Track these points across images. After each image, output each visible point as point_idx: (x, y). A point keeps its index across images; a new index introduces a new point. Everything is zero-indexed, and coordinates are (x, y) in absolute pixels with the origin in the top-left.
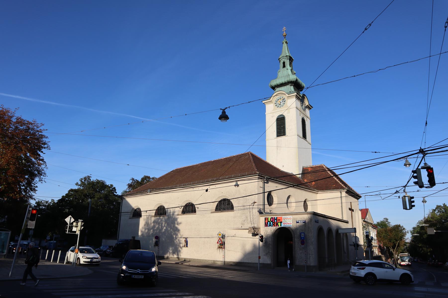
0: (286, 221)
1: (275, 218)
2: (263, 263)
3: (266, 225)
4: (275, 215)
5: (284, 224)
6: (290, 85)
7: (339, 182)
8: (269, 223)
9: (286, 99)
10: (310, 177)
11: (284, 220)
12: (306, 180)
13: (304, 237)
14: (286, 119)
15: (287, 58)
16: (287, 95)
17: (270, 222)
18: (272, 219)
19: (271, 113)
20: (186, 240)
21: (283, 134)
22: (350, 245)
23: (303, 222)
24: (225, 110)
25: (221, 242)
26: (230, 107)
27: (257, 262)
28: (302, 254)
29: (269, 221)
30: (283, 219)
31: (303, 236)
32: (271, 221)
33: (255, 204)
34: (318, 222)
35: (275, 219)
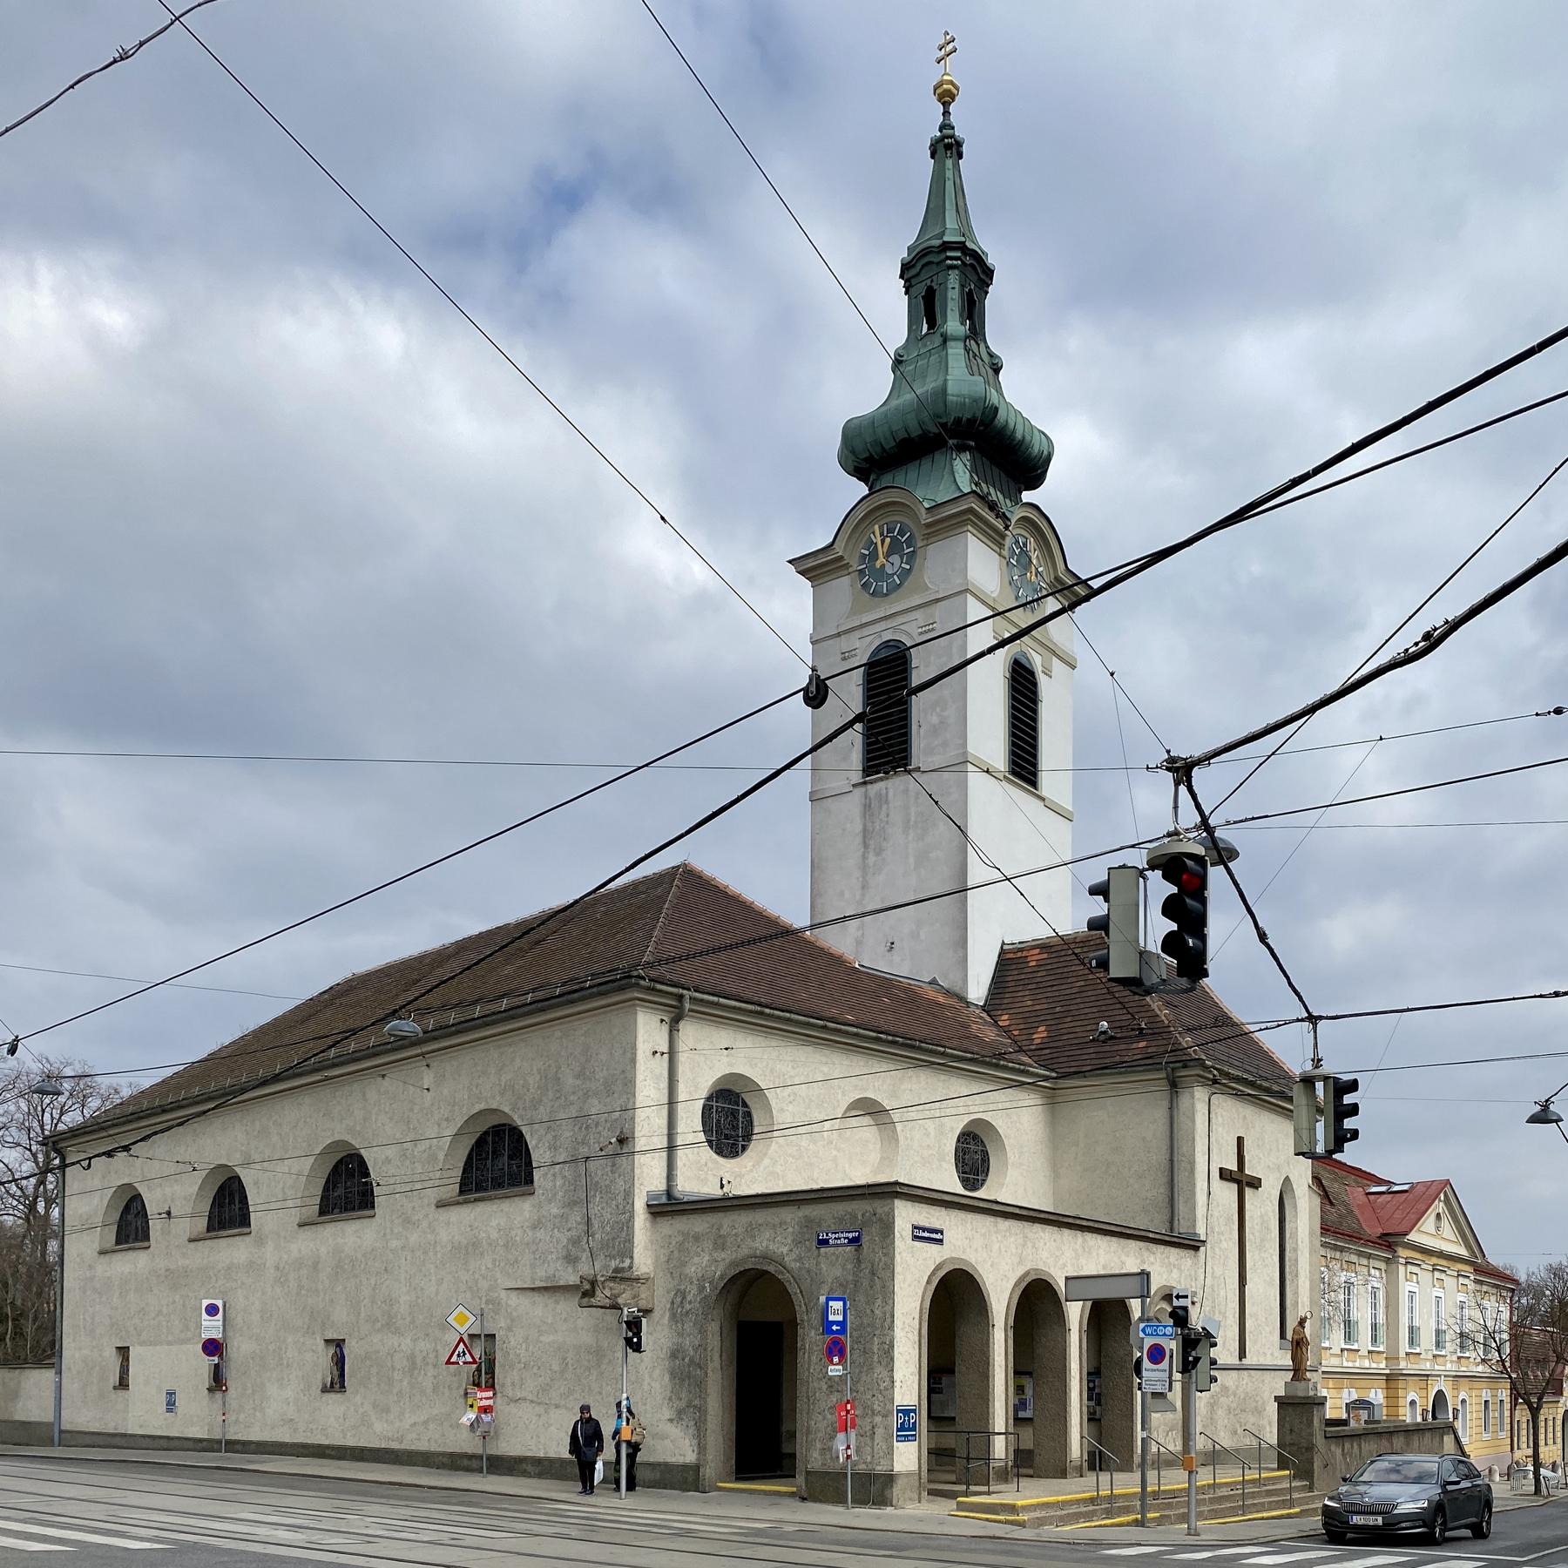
13: (842, 1324)
23: (852, 1241)
31: (840, 1318)
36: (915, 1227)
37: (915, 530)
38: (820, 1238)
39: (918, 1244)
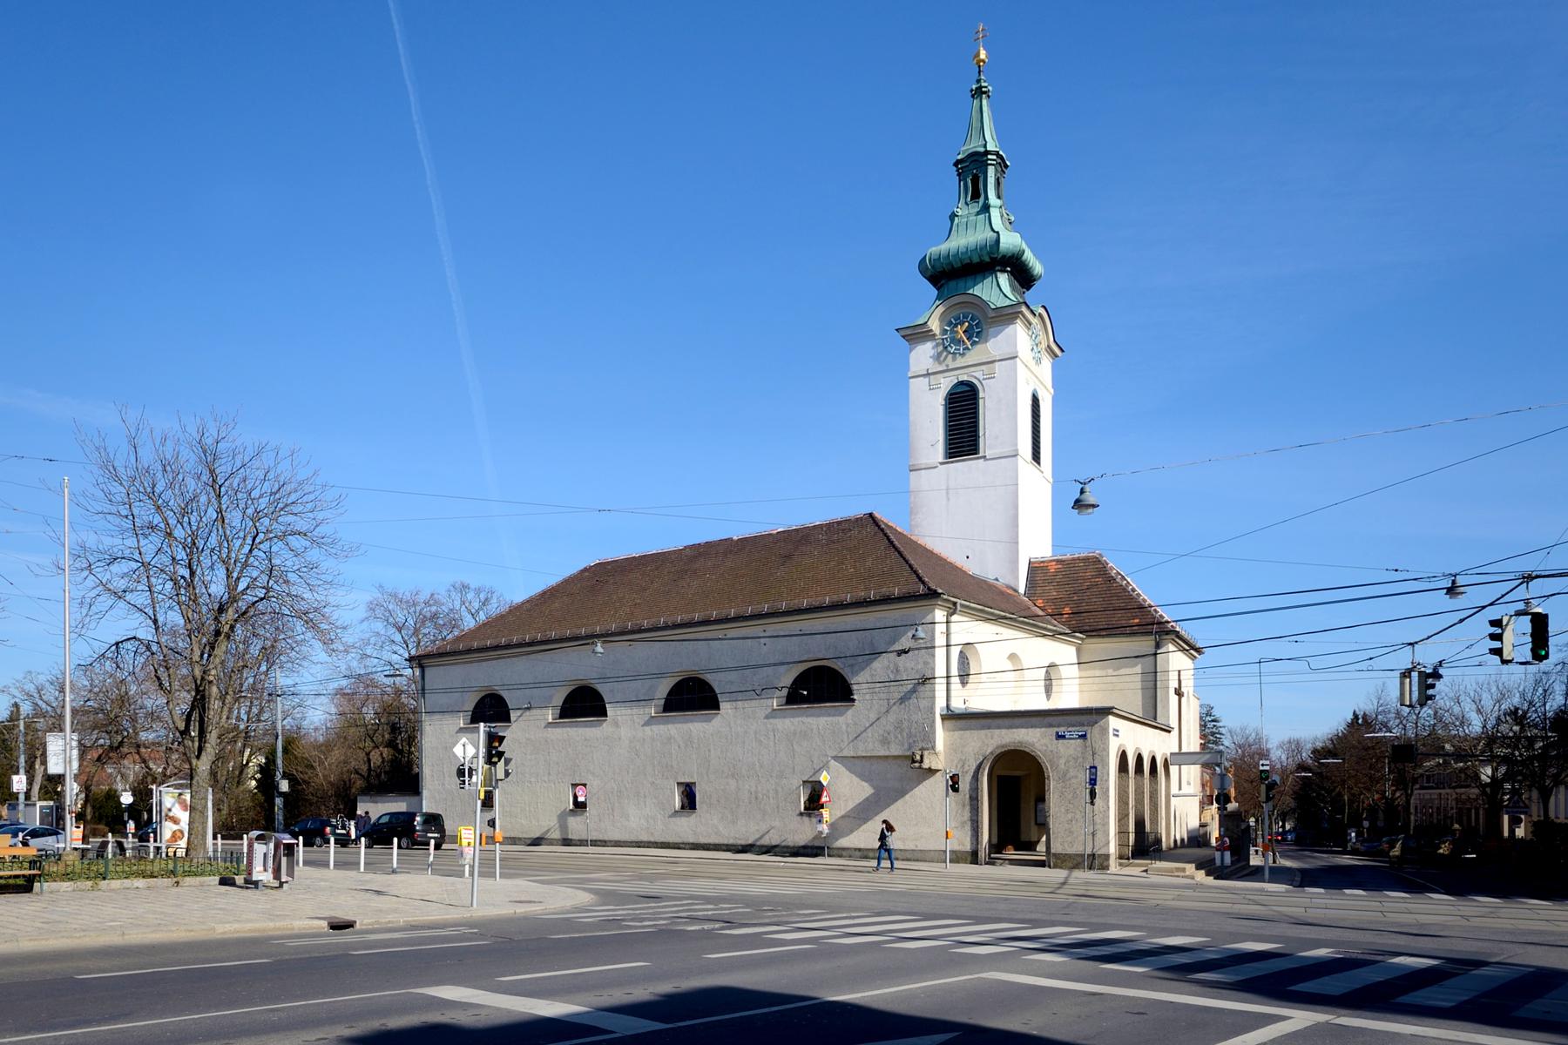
10: (1055, 594)
12: (1041, 601)
20: (688, 789)
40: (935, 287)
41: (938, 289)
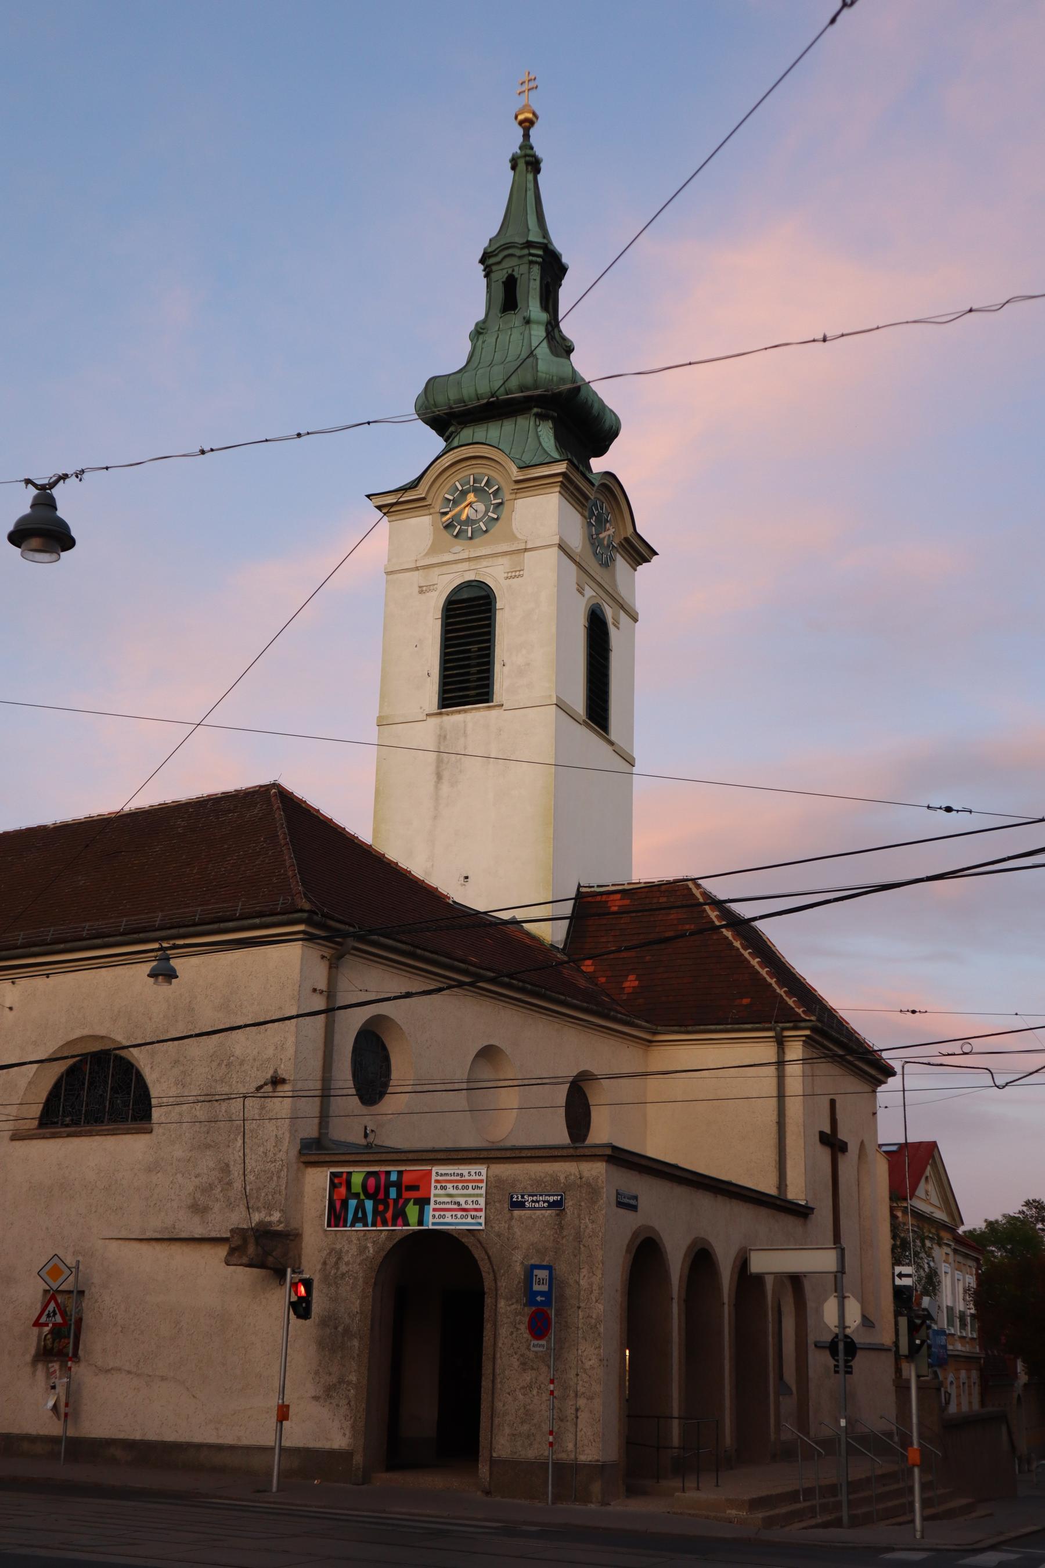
0: (450, 1196)
1: (388, 1173)
2: (307, 1450)
3: (336, 1216)
4: (384, 1157)
5: (437, 1214)
6: (537, 415)
7: (772, 981)
8: (353, 1203)
9: (507, 495)
11: (442, 1188)
13: (547, 1295)
14: (498, 606)
15: (531, 255)
16: (514, 470)
17: (362, 1197)
18: (372, 1181)
19: (417, 569)
21: (478, 695)
22: (817, 1345)
23: (552, 1205)
24: (56, 492)
25: (58, 1319)
26: (83, 471)
27: (267, 1438)
28: (535, 1392)
29: (354, 1191)
30: (433, 1184)
31: (545, 1288)
32: (368, 1196)
33: (280, 1088)
34: (634, 1208)
35: (389, 1184)
36: (618, 1194)
37: (503, 484)
38: (514, 1199)
39: (621, 1211)
40: (442, 437)
41: (446, 441)
